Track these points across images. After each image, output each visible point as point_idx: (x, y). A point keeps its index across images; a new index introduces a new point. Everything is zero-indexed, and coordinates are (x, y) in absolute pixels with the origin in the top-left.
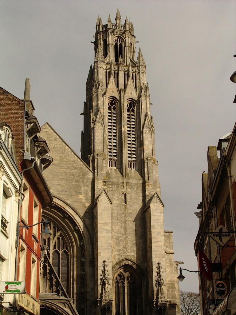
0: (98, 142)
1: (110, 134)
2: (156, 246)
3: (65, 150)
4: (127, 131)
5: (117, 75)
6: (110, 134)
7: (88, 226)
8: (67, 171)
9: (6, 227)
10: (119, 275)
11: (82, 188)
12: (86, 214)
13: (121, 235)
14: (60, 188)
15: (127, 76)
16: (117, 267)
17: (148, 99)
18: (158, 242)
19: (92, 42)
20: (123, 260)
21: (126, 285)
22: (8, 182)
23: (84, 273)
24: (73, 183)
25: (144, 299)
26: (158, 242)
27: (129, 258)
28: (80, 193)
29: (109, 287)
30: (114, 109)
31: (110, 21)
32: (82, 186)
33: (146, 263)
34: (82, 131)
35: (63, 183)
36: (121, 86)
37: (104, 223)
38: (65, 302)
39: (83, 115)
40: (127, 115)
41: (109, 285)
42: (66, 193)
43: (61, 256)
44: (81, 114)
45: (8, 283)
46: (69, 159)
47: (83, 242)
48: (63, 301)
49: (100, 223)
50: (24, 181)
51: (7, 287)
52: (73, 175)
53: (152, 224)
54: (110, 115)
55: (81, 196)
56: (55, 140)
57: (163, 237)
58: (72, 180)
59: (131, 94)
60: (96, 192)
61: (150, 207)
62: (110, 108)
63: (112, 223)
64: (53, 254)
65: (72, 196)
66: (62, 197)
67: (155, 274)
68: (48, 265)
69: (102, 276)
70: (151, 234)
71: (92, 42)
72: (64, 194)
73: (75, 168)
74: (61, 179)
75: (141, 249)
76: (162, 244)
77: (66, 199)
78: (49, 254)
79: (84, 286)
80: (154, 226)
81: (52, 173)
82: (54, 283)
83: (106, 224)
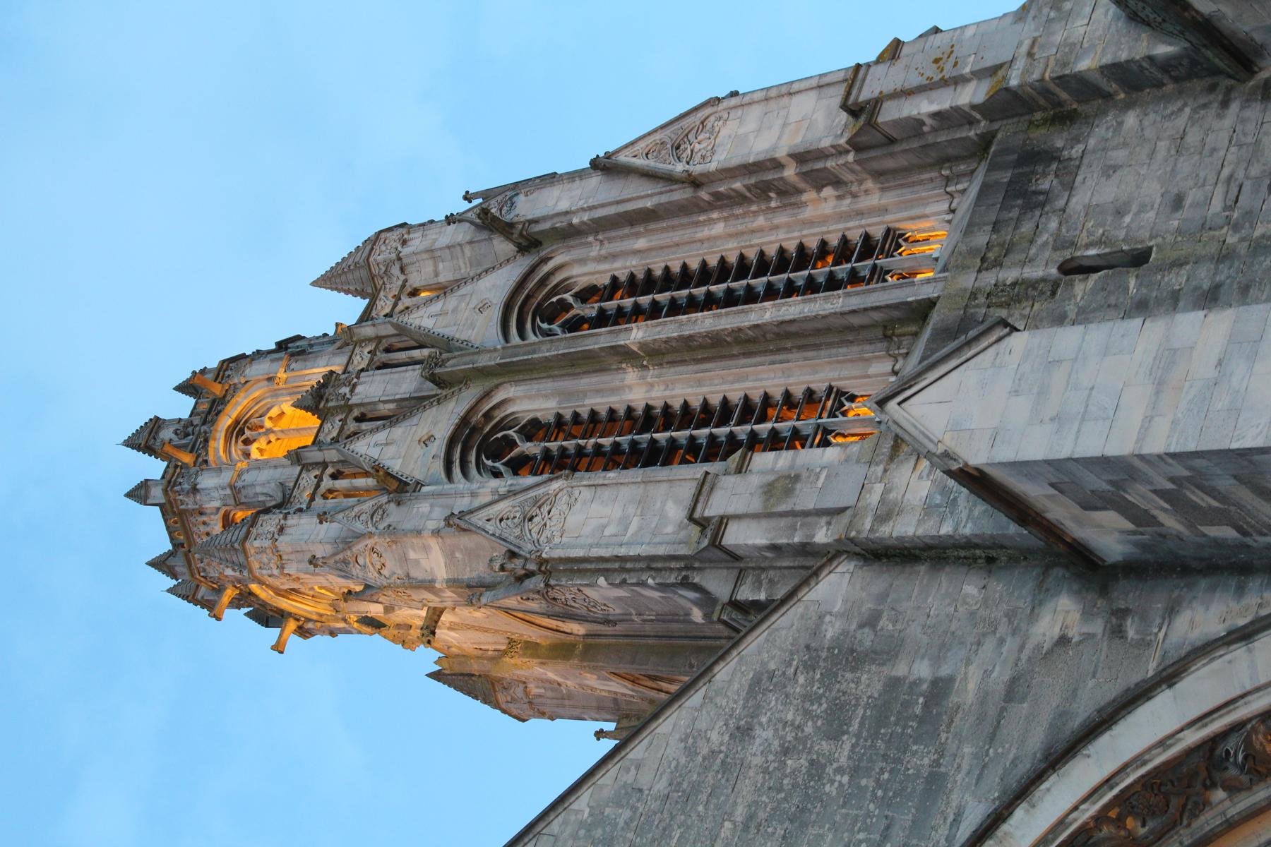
3: (598, 816)
7: (1241, 622)
8: (740, 813)
11: (900, 670)
12: (1131, 633)
24: (843, 760)
28: (940, 689)
32: (886, 671)
37: (1160, 385)
52: (786, 751)
55: (969, 690)
58: (816, 769)
65: (935, 782)
73: (743, 733)
77: (944, 831)
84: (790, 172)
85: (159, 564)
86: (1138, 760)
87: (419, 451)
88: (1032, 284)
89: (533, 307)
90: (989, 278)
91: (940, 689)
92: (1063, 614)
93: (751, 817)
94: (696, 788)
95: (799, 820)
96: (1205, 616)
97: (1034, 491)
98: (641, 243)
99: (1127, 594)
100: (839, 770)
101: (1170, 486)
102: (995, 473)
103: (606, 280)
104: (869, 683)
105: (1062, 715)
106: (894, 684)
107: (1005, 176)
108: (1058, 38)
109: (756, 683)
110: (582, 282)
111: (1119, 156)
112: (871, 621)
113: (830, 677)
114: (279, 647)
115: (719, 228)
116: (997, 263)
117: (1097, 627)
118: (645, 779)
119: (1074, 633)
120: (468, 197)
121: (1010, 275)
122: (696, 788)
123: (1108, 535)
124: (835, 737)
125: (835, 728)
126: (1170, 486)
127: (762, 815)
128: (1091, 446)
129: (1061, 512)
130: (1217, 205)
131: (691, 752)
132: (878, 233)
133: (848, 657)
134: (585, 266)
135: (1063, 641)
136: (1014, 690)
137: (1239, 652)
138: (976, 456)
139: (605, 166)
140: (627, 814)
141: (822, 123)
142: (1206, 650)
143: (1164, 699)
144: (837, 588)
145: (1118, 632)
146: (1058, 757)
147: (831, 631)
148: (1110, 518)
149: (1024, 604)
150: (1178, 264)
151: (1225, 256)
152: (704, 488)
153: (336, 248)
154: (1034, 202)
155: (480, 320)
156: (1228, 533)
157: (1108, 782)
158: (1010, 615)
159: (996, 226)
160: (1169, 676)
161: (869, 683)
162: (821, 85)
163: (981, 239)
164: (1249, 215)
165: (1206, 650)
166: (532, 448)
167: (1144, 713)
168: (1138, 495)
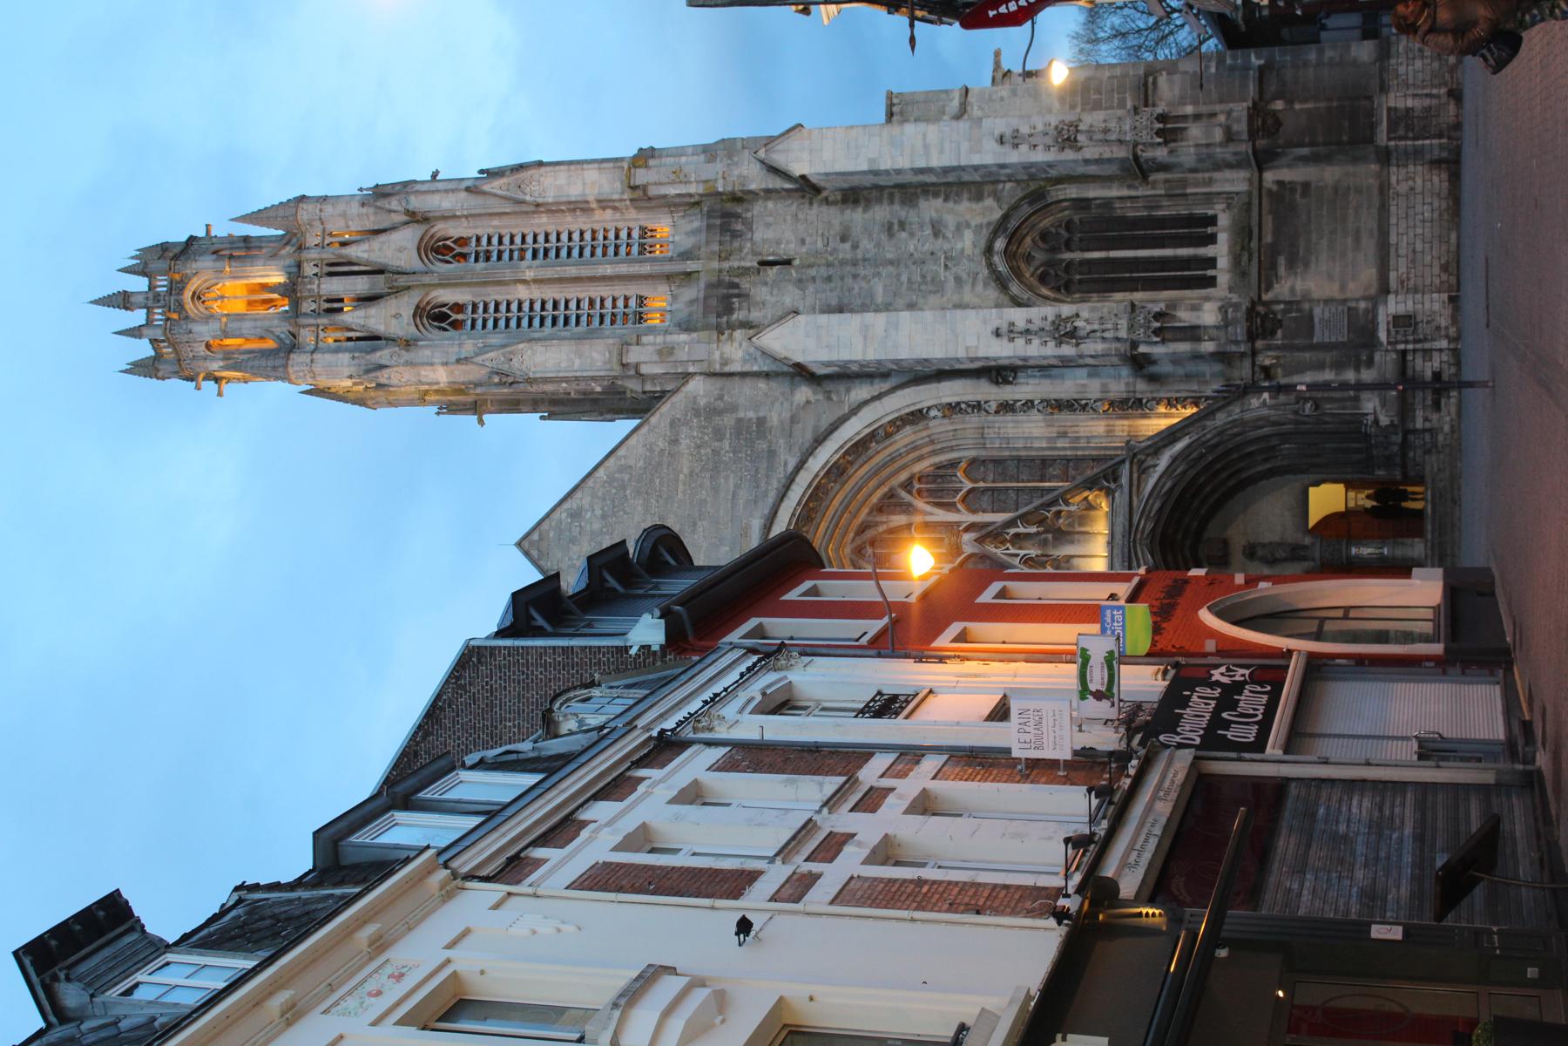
0: (577, 362)
1: (549, 322)
2: (941, 152)
3: (611, 479)
4: (537, 262)
5: (333, 306)
6: (549, 322)
8: (686, 471)
9: (894, 698)
10: (1043, 279)
11: (741, 415)
13: (904, 278)
14: (743, 494)
15: (338, 268)
16: (1015, 288)
17: (418, 187)
18: (926, 147)
19: (220, 394)
20: (990, 265)
21: (1077, 256)
22: (743, 696)
25: (1125, 192)
26: (926, 147)
27: (983, 244)
28: (761, 421)
29: (1085, 314)
30: (459, 308)
31: (134, 333)
33: (1001, 186)
34: (542, 418)
35: (728, 482)
36: (380, 283)
37: (865, 338)
39: (486, 417)
40: (476, 260)
41: (1077, 315)
42: (762, 472)
43: (981, 484)
44: (481, 422)
45: (1084, 692)
46: (641, 463)
47: (929, 408)
48: (1135, 476)
49: (864, 352)
50: (734, 636)
51: (1099, 696)
53: (864, 167)
54: (480, 322)
55: (774, 419)
56: (576, 515)
57: (910, 128)
58: (716, 452)
59: (401, 250)
60: (755, 368)
61: (803, 177)
62: (457, 325)
63: (864, 308)
64: (974, 512)
65: (772, 453)
66: (775, 484)
67: (1039, 156)
68: (1012, 531)
70: (899, 172)
71: (220, 394)
72: (767, 476)
73: (675, 441)
74: (716, 490)
75: (950, 205)
76: (932, 131)
78: (971, 527)
80: (871, 161)
81: (695, 524)
83: (865, 330)
84: (594, 205)
87: (394, 321)
88: (748, 269)
90: (726, 265)
91: (761, 421)
92: (804, 393)
93: (691, 474)
94: (660, 464)
95: (716, 471)
96: (861, 392)
99: (829, 386)
104: (728, 421)
105: (816, 427)
106: (740, 420)
107: (718, 222)
108: (736, 172)
109: (673, 424)
111: (771, 219)
112: (721, 397)
113: (708, 419)
116: (727, 259)
117: (820, 397)
118: (631, 462)
119: (812, 399)
121: (736, 264)
122: (660, 464)
124: (721, 440)
125: (718, 434)
130: (820, 244)
131: (651, 450)
133: (712, 412)
135: (808, 402)
136: (794, 420)
137: (877, 403)
140: (626, 477)
142: (866, 403)
143: (854, 420)
144: (696, 386)
145: (829, 398)
146: (819, 441)
147: (702, 402)
149: (787, 390)
150: (811, 266)
151: (829, 265)
154: (736, 235)
155: (403, 256)
158: (783, 394)
159: (721, 243)
160: (854, 411)
161: (728, 421)
163: (716, 247)
164: (835, 250)
165: (866, 403)
167: (847, 425)
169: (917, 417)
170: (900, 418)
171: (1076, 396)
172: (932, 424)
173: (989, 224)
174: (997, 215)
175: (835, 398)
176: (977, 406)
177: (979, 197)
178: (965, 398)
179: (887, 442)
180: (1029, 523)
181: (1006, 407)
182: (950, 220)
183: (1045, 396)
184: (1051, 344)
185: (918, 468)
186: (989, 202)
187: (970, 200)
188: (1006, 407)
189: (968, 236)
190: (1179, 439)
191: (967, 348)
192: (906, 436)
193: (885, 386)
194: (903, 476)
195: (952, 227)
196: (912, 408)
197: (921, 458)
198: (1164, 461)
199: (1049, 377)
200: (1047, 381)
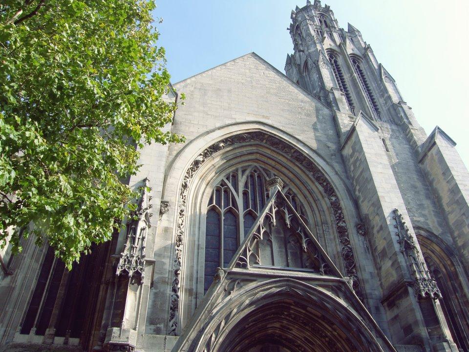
23: (349, 246)
38: (334, 286)
42: (294, 127)
47: (336, 196)
48: (330, 284)
68: (286, 211)
69: (399, 235)
79: (354, 270)
82: (305, 246)
84: (386, 95)
85: (297, 8)
86: (315, 161)
89: (355, 58)
92: (333, 147)
96: (338, 167)
97: (353, 138)
98: (368, 73)
100: (301, 117)
101: (359, 159)
102: (355, 132)
103: (361, 69)
110: (360, 65)
114: (288, 29)
115: (374, 85)
117: (333, 152)
120: (369, 45)
123: (347, 151)
126: (359, 159)
127: (291, 106)
128: (363, 146)
129: (350, 143)
132: (379, 110)
134: (363, 66)
135: (328, 147)
137: (334, 173)
138: (357, 128)
139: (380, 66)
141: (395, 99)
145: (332, 155)
148: (351, 151)
152: (337, 89)
153: (356, 26)
156: (352, 168)
157: (310, 157)
162: (401, 98)
166: (333, 61)
168: (356, 154)
169: (329, 190)
170: (328, 183)
171: (357, 265)
172: (326, 199)
173: (430, 228)
174: (435, 232)
175: (333, 157)
176: (340, 218)
177: (440, 225)
178: (345, 212)
179: (313, 179)
180: (291, 221)
181: (342, 231)
182: (426, 212)
183: (354, 251)
184: (397, 238)
185: (300, 197)
186: (440, 230)
187: (438, 221)
188: (342, 231)
189: (422, 219)
190: (359, 314)
191: (384, 197)
192: (317, 188)
193: (343, 177)
194: (295, 190)
195: (423, 212)
196: (334, 188)
197: (305, 197)
198: (342, 302)
199: (366, 252)
200: (363, 251)
